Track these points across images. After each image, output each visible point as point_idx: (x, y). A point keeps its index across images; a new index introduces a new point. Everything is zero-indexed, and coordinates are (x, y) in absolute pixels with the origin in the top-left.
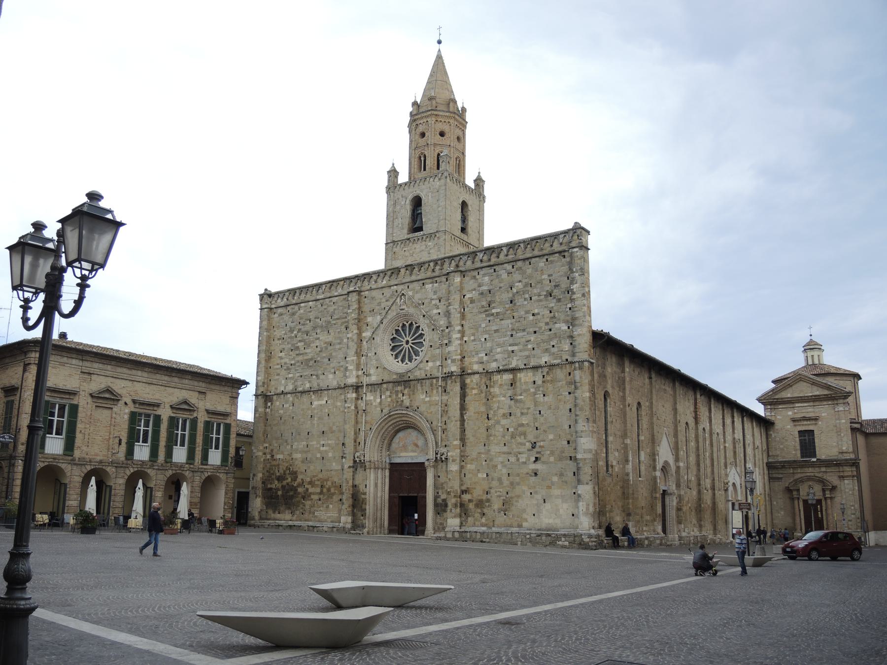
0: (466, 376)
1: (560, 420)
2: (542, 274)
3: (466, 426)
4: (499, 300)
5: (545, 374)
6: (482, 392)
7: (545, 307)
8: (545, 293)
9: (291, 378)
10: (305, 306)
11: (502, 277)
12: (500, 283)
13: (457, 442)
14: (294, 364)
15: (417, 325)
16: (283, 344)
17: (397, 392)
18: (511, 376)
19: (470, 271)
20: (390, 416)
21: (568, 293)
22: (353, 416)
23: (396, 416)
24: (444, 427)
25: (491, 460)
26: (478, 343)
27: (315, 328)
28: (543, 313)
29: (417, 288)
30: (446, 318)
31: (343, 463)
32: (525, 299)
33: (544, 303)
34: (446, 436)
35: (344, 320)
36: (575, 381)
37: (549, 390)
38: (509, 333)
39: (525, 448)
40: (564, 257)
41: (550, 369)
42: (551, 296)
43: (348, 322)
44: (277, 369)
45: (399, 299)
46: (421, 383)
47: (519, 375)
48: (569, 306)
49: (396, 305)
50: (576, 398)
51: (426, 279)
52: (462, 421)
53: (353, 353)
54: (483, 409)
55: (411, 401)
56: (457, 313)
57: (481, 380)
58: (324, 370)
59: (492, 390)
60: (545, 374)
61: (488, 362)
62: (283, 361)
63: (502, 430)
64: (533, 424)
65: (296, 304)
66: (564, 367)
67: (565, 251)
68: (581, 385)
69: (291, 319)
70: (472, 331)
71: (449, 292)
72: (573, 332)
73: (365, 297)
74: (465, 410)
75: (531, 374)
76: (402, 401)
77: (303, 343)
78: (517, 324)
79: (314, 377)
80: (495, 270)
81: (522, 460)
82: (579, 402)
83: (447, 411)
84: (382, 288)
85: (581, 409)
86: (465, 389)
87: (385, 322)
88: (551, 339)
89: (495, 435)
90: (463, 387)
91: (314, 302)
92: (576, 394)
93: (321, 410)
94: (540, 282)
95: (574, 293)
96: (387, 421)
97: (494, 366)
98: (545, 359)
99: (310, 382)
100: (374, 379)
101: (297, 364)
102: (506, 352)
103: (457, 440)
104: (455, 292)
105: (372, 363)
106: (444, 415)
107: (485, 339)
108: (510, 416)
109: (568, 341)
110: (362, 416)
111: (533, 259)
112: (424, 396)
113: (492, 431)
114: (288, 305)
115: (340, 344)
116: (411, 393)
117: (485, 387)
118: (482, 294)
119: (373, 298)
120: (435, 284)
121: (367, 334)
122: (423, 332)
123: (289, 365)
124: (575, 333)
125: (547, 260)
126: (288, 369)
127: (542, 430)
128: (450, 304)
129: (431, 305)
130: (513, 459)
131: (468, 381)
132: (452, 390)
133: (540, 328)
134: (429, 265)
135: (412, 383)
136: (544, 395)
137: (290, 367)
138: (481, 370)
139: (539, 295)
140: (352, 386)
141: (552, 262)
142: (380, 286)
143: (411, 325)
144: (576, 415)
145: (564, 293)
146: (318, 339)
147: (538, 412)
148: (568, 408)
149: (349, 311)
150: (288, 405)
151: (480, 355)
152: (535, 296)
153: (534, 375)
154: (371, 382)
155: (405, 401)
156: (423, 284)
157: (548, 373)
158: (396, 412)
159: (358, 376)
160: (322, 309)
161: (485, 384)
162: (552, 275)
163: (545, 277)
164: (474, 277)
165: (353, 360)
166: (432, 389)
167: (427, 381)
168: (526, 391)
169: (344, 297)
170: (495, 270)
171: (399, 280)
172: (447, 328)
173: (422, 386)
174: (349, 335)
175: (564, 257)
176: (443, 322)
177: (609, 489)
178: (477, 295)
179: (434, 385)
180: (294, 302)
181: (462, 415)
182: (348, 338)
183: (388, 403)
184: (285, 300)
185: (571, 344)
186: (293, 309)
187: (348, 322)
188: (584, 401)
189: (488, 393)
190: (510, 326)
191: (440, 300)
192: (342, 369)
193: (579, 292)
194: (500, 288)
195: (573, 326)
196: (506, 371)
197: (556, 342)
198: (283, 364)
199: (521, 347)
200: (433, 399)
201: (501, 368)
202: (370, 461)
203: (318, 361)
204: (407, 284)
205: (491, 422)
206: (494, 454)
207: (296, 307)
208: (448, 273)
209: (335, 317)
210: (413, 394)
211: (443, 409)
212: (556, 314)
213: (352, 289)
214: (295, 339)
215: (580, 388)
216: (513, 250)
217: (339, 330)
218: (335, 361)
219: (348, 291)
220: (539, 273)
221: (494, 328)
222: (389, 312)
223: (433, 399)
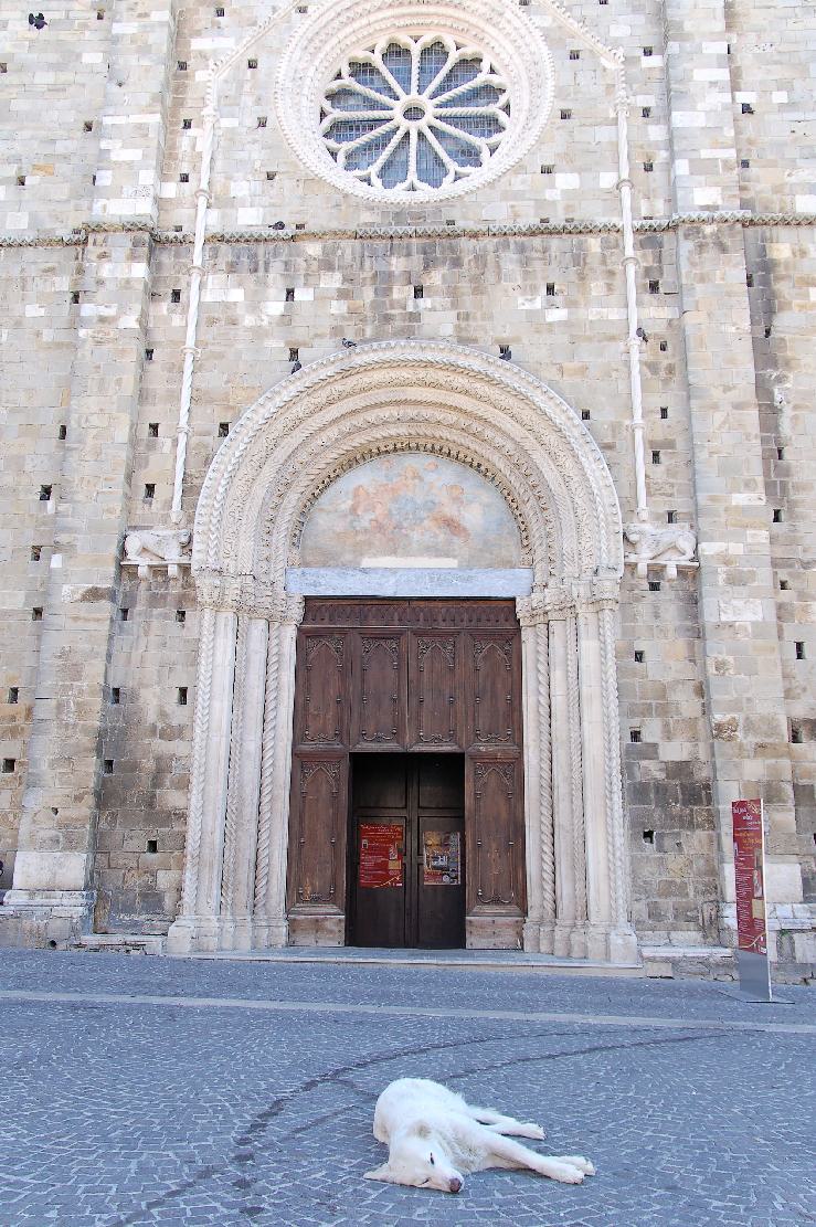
17: (384, 282)
20: (345, 373)
23: (378, 376)
24: (661, 430)
46: (522, 249)
52: (770, 413)
53: (145, 99)
70: (779, 72)
76: (415, 317)
86: (766, 282)
90: (761, 275)
100: (250, 218)
105: (243, 155)
116: (465, 286)
135: (465, 244)
140: (128, 228)
155: (426, 318)
165: (142, 129)
166: (582, 277)
172: (648, 52)
179: (594, 261)
181: (763, 388)
183: (325, 326)
200: (593, 314)
210: (478, 290)
211: (645, 357)
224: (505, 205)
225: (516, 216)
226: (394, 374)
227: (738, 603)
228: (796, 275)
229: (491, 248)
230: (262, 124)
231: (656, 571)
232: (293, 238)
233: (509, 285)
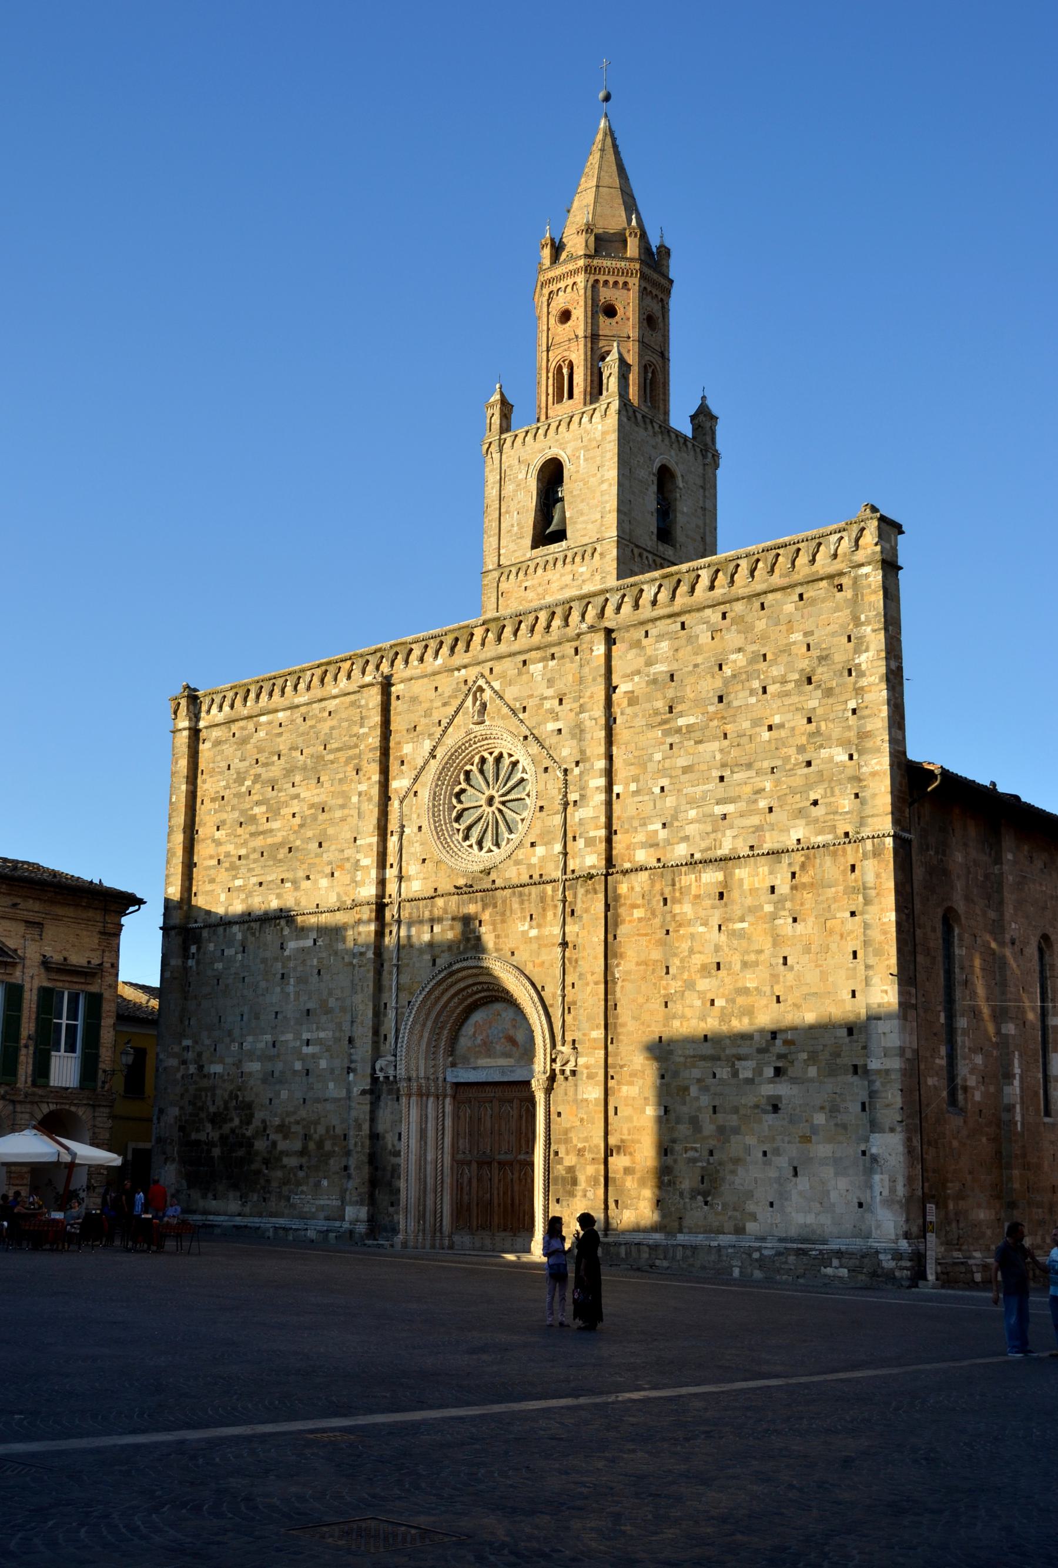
0: (619, 877)
1: (830, 979)
2: (791, 631)
3: (618, 995)
4: (692, 696)
5: (797, 869)
6: (653, 913)
7: (797, 709)
8: (796, 676)
9: (240, 889)
10: (270, 723)
11: (700, 642)
12: (696, 654)
13: (599, 1034)
14: (247, 857)
15: (513, 759)
16: (221, 809)
18: (720, 876)
19: (628, 628)
20: (451, 974)
21: (850, 674)
22: (371, 974)
23: (464, 973)
25: (676, 1074)
26: (646, 798)
27: (289, 772)
28: (792, 724)
29: (510, 673)
30: (574, 742)
31: (349, 1083)
32: (752, 692)
33: (795, 699)
34: (575, 1019)
35: (351, 752)
36: (864, 883)
37: (807, 906)
38: (716, 774)
39: (751, 1046)
40: (840, 588)
41: (807, 857)
42: (809, 681)
43: (359, 756)
44: (209, 868)
45: (470, 698)
46: (521, 894)
47: (741, 873)
48: (852, 704)
49: (464, 714)
50: (866, 926)
51: (531, 650)
54: (656, 954)
55: (498, 937)
56: (598, 728)
57: (653, 885)
58: (309, 869)
59: (677, 909)
60: (797, 869)
61: (668, 842)
62: (222, 849)
63: (698, 1003)
64: (767, 989)
65: (249, 717)
66: (840, 852)
67: (841, 574)
68: (878, 894)
69: (239, 753)
71: (581, 680)
72: (860, 767)
73: (398, 697)
74: (615, 956)
75: (766, 869)
77: (263, 808)
78: (734, 753)
79: (288, 885)
80: (683, 624)
81: (746, 1074)
82: (875, 934)
83: (576, 961)
84: (434, 674)
85: (878, 953)
87: (440, 753)
88: (809, 786)
89: (683, 1017)
91: (288, 713)
92: (867, 916)
93: (304, 962)
94: (786, 650)
95: (861, 674)
96: (444, 986)
97: (681, 851)
98: (798, 832)
99: (279, 896)
101: (252, 857)
102: (709, 819)
103: (598, 1027)
104: (594, 680)
105: (412, 850)
106: (572, 969)
107: (662, 789)
108: (718, 968)
109: (851, 790)
110: (391, 973)
111: (770, 596)
112: (526, 927)
113: (675, 1007)
114: (234, 721)
115: (343, 807)
116: (498, 918)
117: (662, 904)
118: (655, 681)
119: (414, 700)
120: (551, 663)
121: (399, 784)
122: (525, 776)
123: (236, 859)
124: (864, 770)
125: (801, 596)
126: (233, 867)
127: (790, 1002)
128: (582, 709)
129: (542, 711)
130: (724, 1073)
131: (623, 889)
132: (587, 910)
133: (787, 759)
134: (537, 618)
135: (499, 893)
136: (795, 920)
137: (238, 862)
138: (653, 863)
139: (784, 682)
141: (813, 601)
142: (429, 670)
143: (499, 759)
144: (868, 967)
145: (841, 675)
146: (297, 796)
147: (781, 961)
148: (851, 951)
149: (362, 731)
150: (232, 952)
151: (651, 828)
152: (774, 683)
153: (771, 873)
154: (411, 896)
156: (525, 662)
157: (803, 866)
158: (465, 964)
159: (382, 883)
160: (304, 727)
161: (662, 894)
162: (811, 633)
163: (797, 637)
164: (637, 644)
166: (544, 909)
167: (533, 889)
168: (753, 910)
169: (352, 697)
170: (683, 624)
171: (469, 654)
172: (577, 763)
173: (522, 902)
174: (363, 787)
175: (840, 588)
176: (567, 751)
177: (955, 1143)
178: (644, 685)
179: (549, 900)
180: (245, 712)
182: (360, 794)
184: (226, 708)
185: (857, 796)
186: (243, 728)
187: (359, 756)
188: (885, 933)
189: (668, 917)
190: (718, 757)
191: (561, 700)
192: (348, 865)
193: (875, 670)
194: (696, 666)
195: (861, 753)
196: (705, 862)
197: (823, 793)
198: (222, 858)
199: (742, 805)
200: (546, 931)
201: (698, 856)
202: (409, 1079)
203: (297, 848)
204: (489, 665)
205: (674, 986)
206: (682, 1059)
207: (251, 725)
208: (579, 635)
209: (335, 746)
210: (503, 921)
212: (823, 724)
213: (368, 679)
214: (247, 798)
215: (876, 900)
216: (725, 574)
217: (341, 776)
218: (333, 847)
219: (361, 682)
220: (784, 628)
221: (682, 762)
222: (450, 730)
223: (546, 931)
224: (514, 868)
225: (520, 874)
226: (470, 971)
227: (590, 1088)
228: (628, 902)
229: (508, 896)
230: (420, 828)
231: (563, 1072)
232: (433, 898)
233: (516, 916)
